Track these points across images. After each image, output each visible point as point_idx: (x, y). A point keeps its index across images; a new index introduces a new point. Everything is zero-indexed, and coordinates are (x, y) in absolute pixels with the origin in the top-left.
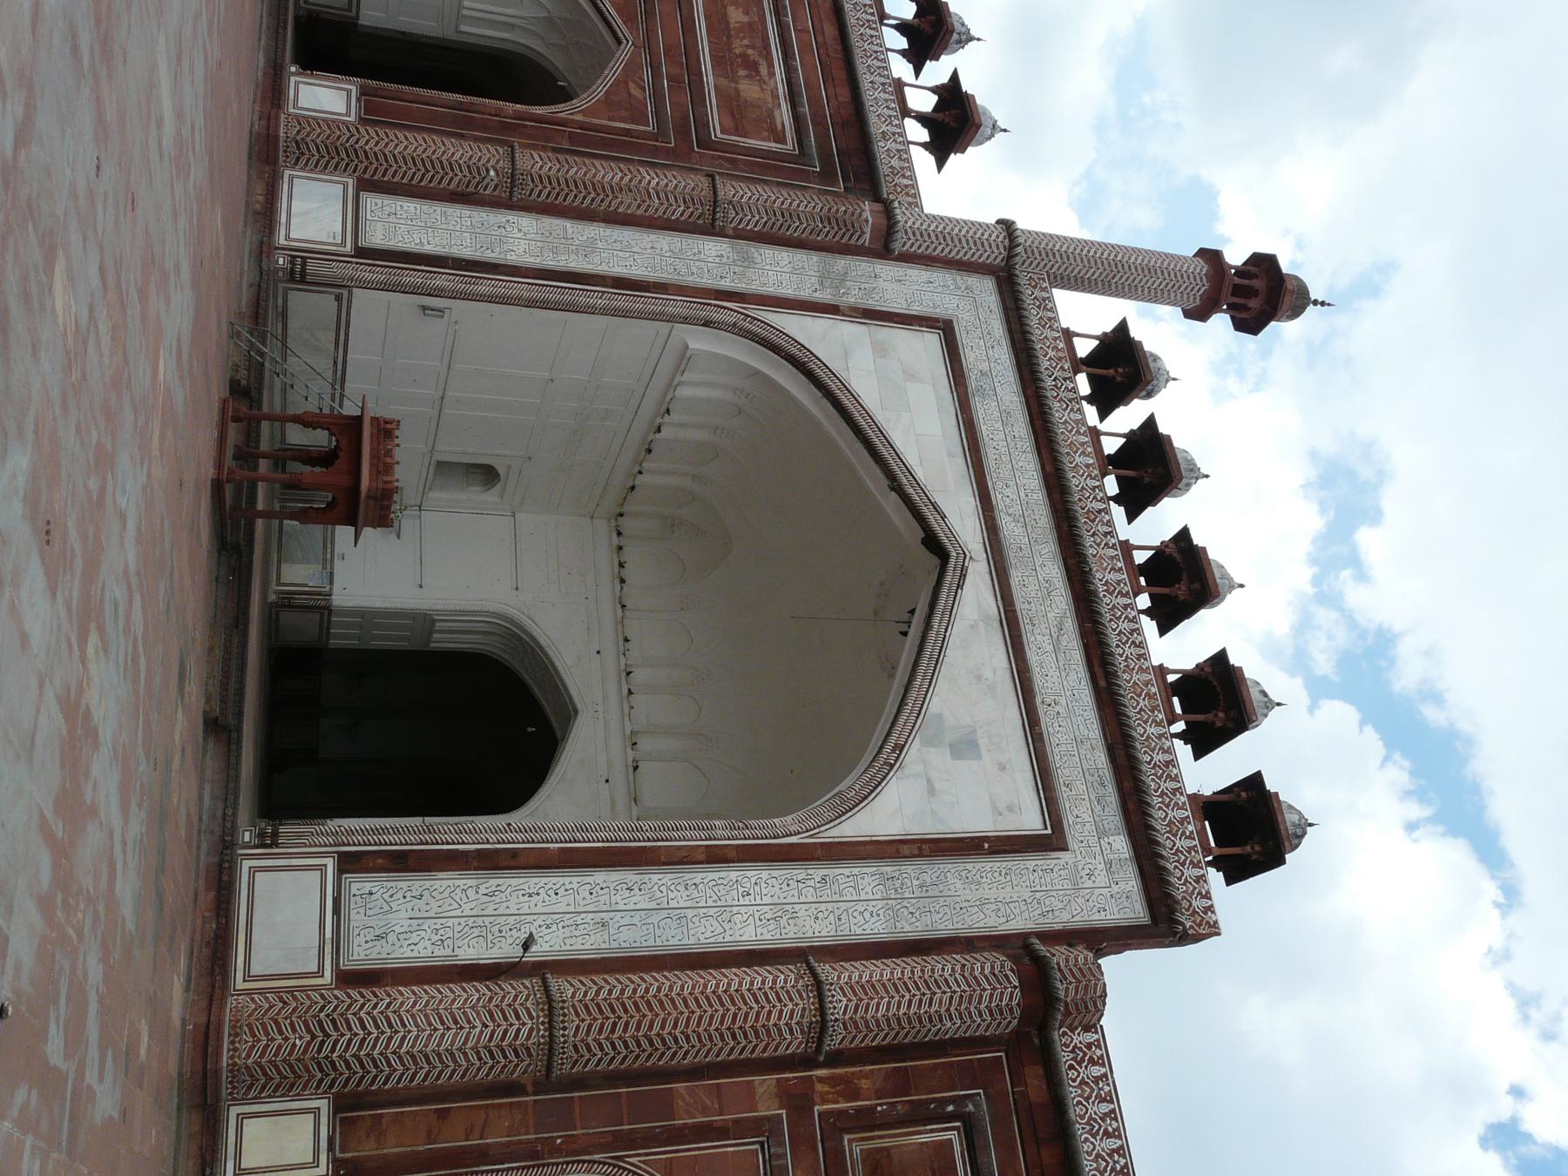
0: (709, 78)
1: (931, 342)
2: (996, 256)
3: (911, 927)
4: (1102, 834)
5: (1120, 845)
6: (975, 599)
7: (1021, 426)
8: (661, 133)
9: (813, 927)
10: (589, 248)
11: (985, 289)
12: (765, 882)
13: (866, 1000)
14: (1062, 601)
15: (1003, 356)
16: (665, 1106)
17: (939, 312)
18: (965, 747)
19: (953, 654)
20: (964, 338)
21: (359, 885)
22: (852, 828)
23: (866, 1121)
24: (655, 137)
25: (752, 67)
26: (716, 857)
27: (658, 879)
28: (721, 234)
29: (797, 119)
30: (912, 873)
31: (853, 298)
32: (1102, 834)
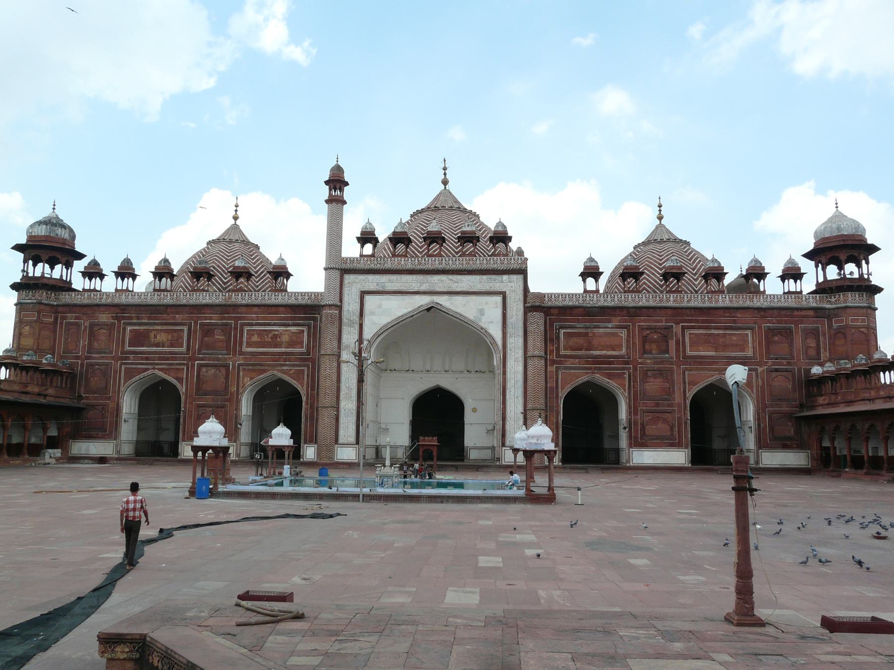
0: (283, 350)
1: (368, 298)
2: (337, 274)
3: (521, 333)
5: (505, 277)
6: (444, 301)
8: (308, 366)
9: (520, 354)
10: (349, 388)
11: (348, 278)
12: (510, 363)
13: (537, 346)
15: (371, 277)
16: (551, 388)
17: (358, 294)
18: (482, 312)
20: (366, 289)
22: (500, 342)
23: (558, 349)
24: (308, 368)
25: (275, 336)
26: (504, 373)
27: (509, 385)
28: (340, 353)
30: (510, 330)
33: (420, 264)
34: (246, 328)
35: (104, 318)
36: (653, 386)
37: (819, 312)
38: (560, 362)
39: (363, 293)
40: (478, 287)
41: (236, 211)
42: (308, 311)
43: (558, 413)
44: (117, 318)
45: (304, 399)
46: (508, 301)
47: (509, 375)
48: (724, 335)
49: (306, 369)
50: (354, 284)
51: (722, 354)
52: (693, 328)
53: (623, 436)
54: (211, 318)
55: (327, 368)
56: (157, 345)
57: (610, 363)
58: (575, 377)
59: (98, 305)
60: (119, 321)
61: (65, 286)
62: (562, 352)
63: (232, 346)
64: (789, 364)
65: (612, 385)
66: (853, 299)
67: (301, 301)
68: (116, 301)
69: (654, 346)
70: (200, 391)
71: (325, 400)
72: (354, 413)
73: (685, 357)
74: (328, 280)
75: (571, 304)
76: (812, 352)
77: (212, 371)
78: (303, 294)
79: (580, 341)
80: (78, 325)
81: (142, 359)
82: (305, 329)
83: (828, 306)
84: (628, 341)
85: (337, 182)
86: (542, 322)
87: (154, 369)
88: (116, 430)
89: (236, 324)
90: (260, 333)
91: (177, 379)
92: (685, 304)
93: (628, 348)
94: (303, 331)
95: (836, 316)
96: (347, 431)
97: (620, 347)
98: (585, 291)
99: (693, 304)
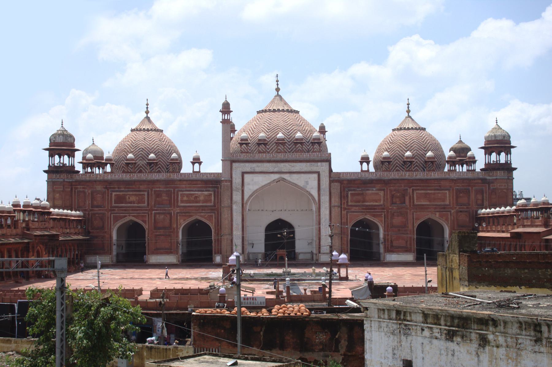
0: (201, 204)
1: (246, 176)
2: (229, 163)
3: (328, 193)
4: (318, 166)
5: (319, 164)
7: (259, 164)
9: (327, 205)
12: (322, 210)
13: (336, 201)
14: (287, 164)
15: (247, 164)
18: (307, 183)
19: (295, 182)
20: (245, 171)
21: (322, 251)
22: (317, 199)
23: (347, 202)
25: (196, 197)
26: (319, 215)
27: (322, 221)
29: (206, 191)
30: (322, 192)
31: (240, 187)
32: (318, 166)
33: (273, 157)
34: (180, 193)
35: (99, 188)
36: (397, 221)
37: (484, 181)
38: (349, 209)
39: (243, 173)
41: (147, 108)
42: (213, 183)
43: (347, 236)
44: (106, 188)
45: (213, 231)
46: (321, 176)
47: (322, 216)
48: (434, 194)
49: (214, 214)
50: (238, 168)
52: (418, 190)
53: (382, 246)
54: (159, 188)
55: (225, 215)
56: (131, 203)
57: (375, 209)
59: (95, 181)
60: (108, 190)
61: (71, 170)
62: (350, 204)
64: (467, 208)
65: (376, 220)
66: (500, 174)
67: (209, 178)
68: (106, 178)
69: (398, 200)
70: (156, 228)
71: (225, 230)
72: (241, 237)
73: (414, 205)
74: (224, 166)
75: (354, 178)
76: (479, 202)
77: (162, 217)
78: (211, 174)
79: (359, 198)
80: (84, 192)
81: (122, 210)
82: (212, 193)
83: (488, 178)
84: (384, 197)
85: (226, 109)
86: (339, 187)
87: (130, 216)
88: (111, 250)
89: (174, 191)
90: (188, 196)
91: (143, 221)
92: (414, 177)
93: (384, 201)
94: (211, 194)
95: (493, 183)
97: (380, 200)
98: (362, 171)
99: (418, 177)
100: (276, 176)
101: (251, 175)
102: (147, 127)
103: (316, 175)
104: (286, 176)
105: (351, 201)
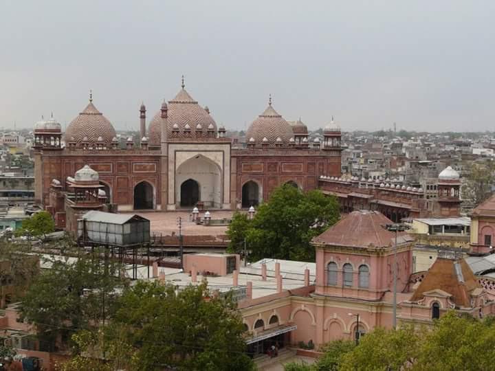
5: (224, 145)
6: (203, 154)
11: (170, 145)
13: (234, 168)
17: (173, 153)
18: (216, 158)
20: (176, 149)
22: (222, 168)
31: (173, 160)
39: (176, 151)
40: (215, 149)
50: (172, 148)
51: (293, 171)
55: (164, 178)
58: (245, 179)
63: (129, 171)
66: (334, 154)
77: (122, 180)
79: (248, 168)
96: (171, 200)
100: (196, 154)
101: (180, 153)
102: (92, 112)
103: (222, 153)
104: (203, 154)
105: (244, 170)
